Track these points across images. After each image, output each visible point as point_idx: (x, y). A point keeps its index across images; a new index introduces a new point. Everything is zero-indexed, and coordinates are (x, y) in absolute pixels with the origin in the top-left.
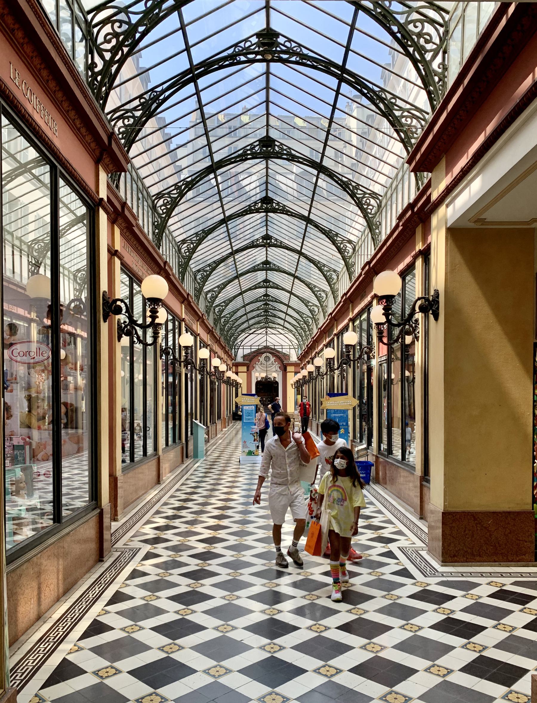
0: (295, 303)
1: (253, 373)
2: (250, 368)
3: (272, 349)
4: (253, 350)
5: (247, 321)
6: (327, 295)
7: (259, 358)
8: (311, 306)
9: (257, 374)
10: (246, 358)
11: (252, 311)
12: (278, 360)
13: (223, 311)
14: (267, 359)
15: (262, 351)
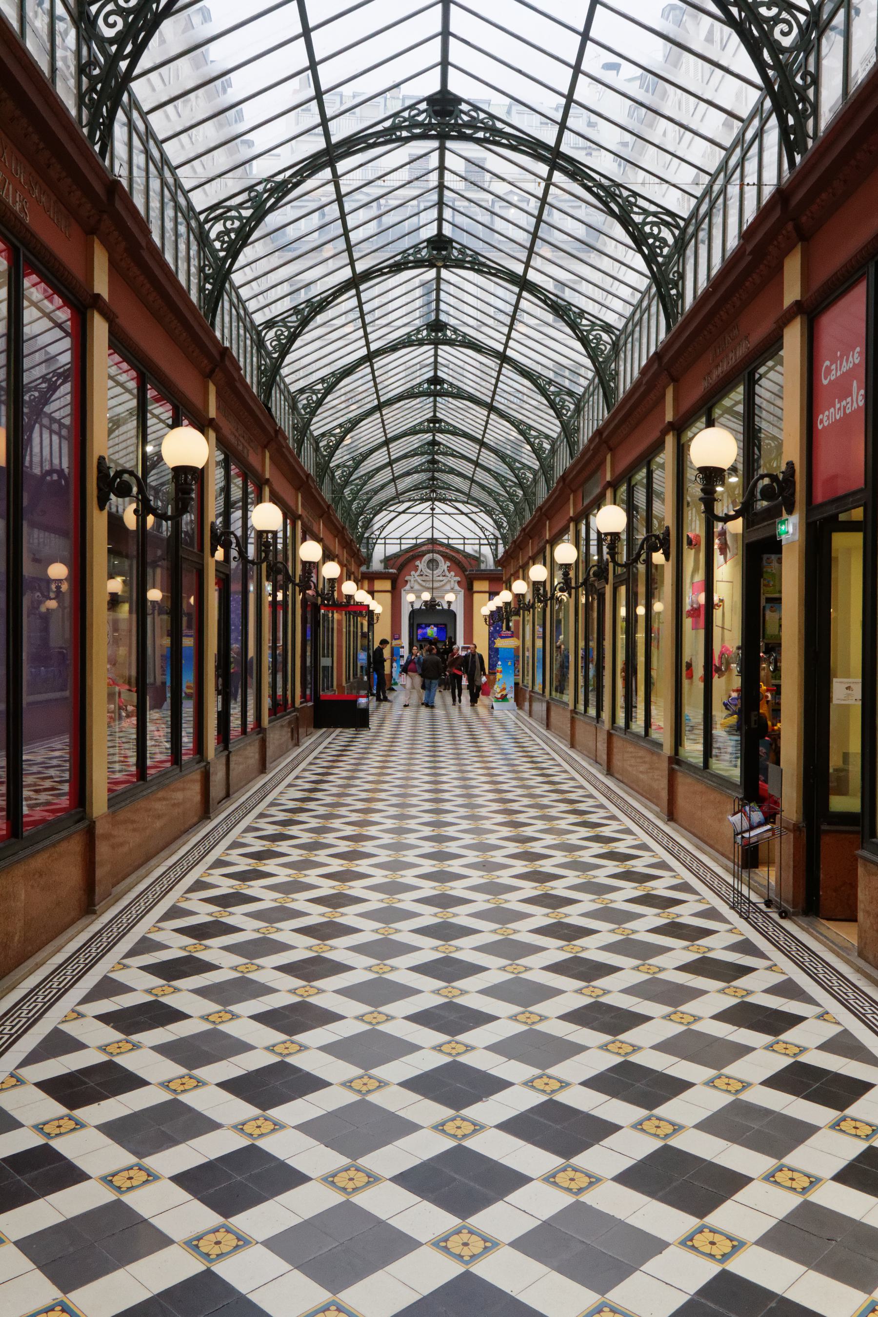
0: (489, 459)
2: (400, 581)
3: (442, 544)
4: (404, 547)
7: (417, 563)
8: (519, 469)
10: (392, 562)
11: (408, 474)
15: (424, 548)
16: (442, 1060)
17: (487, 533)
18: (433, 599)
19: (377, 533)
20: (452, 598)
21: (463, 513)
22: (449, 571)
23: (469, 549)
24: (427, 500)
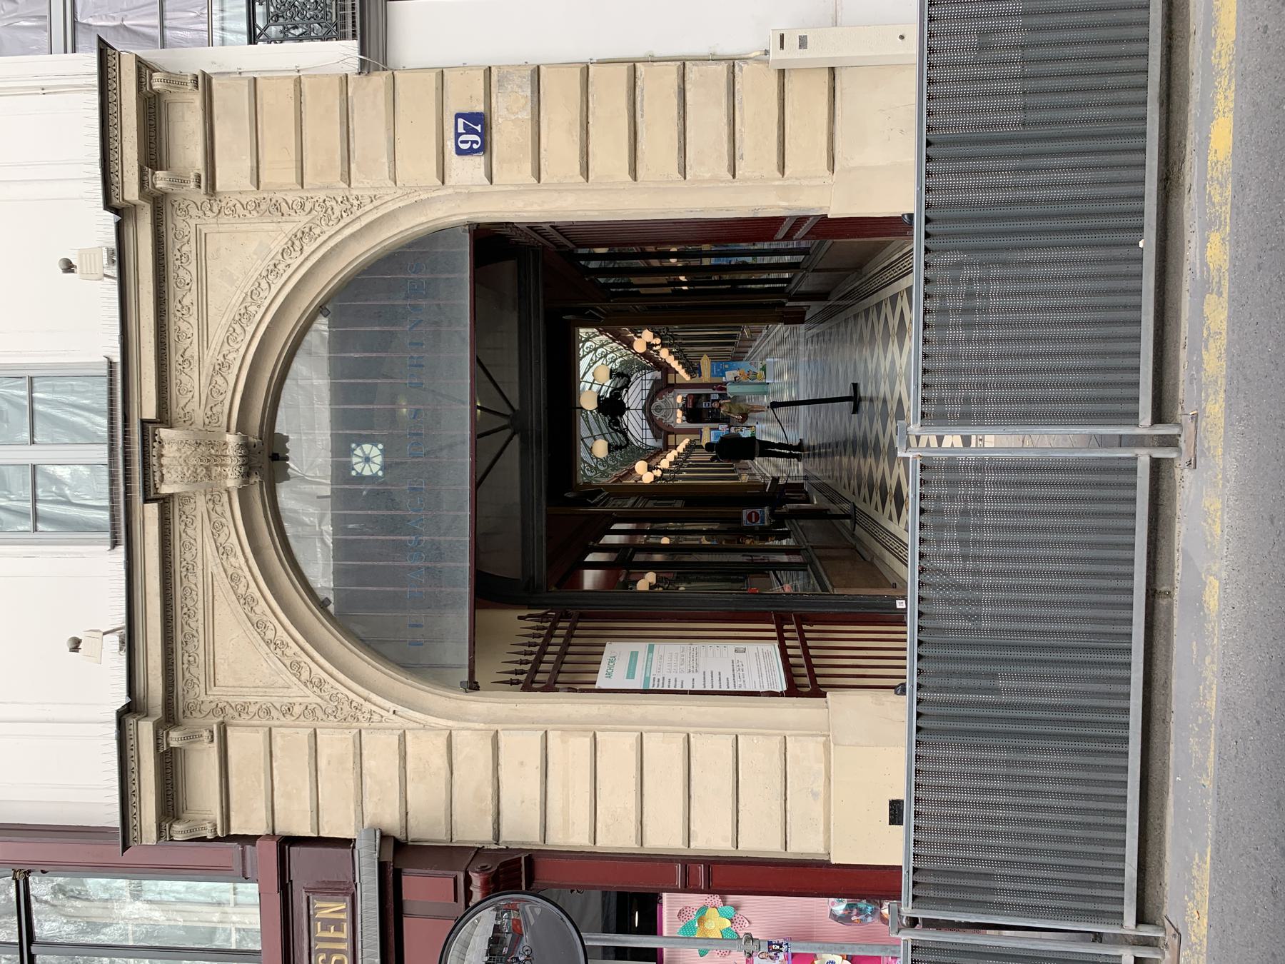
1: (677, 427)
2: (669, 430)
4: (648, 427)
9: (679, 421)
11: (600, 427)
14: (659, 409)
22: (662, 398)
23: (648, 387)
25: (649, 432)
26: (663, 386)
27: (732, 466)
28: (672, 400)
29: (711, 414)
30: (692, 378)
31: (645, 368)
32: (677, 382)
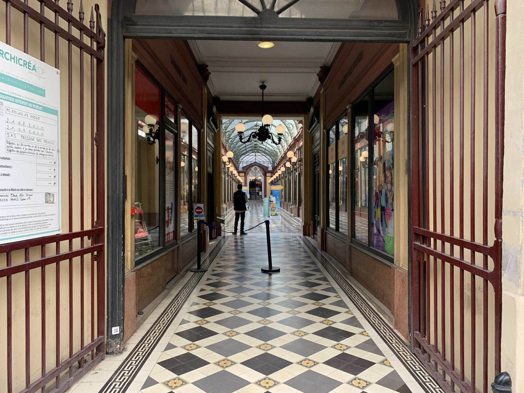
3: (258, 164)
4: (248, 164)
5: (246, 149)
6: (293, 127)
9: (250, 178)
12: (262, 170)
13: (231, 135)
14: (256, 169)
15: (253, 164)
16: (261, 352)
17: (270, 160)
18: (256, 179)
19: (241, 160)
20: (260, 178)
21: (263, 155)
23: (265, 165)
24: (254, 152)
25: (246, 165)
26: (265, 171)
27: (230, 200)
28: (259, 175)
29: (253, 192)
30: (269, 183)
31: (274, 163)
32: (267, 177)
